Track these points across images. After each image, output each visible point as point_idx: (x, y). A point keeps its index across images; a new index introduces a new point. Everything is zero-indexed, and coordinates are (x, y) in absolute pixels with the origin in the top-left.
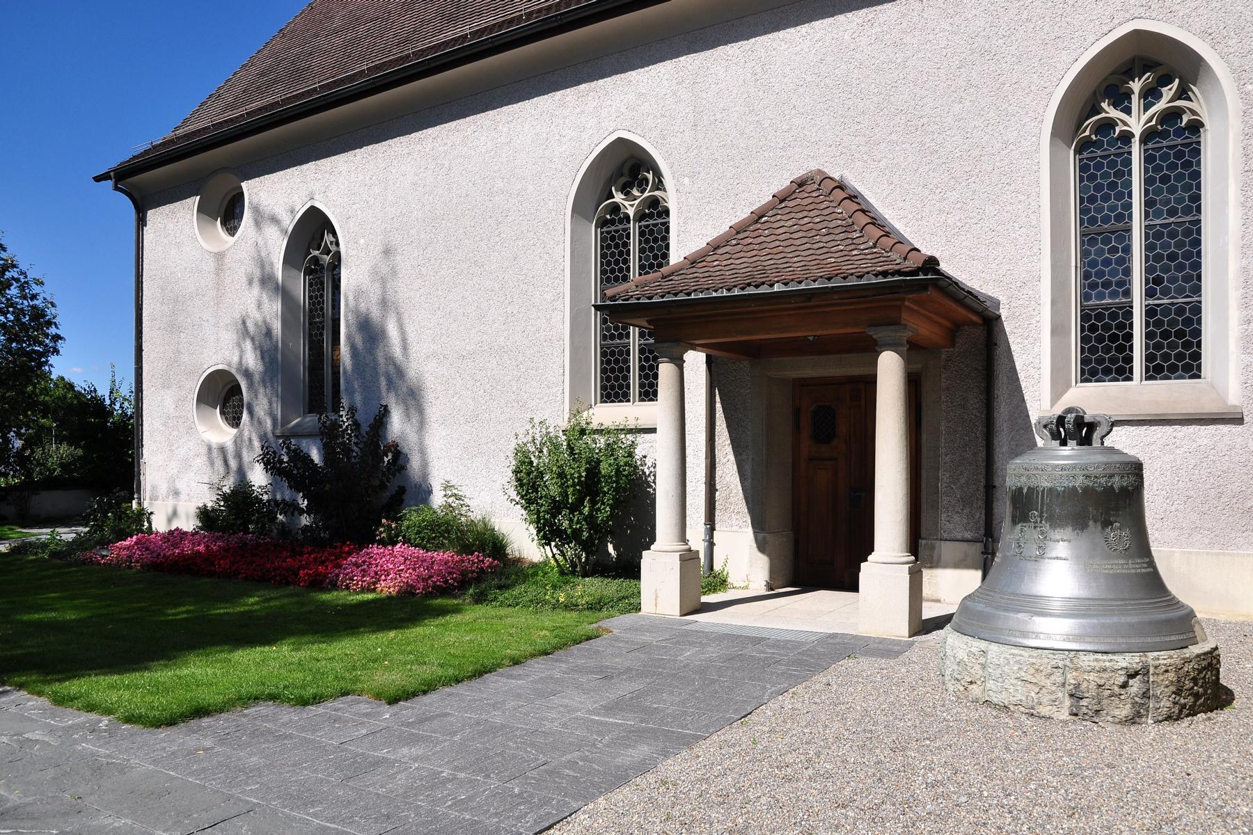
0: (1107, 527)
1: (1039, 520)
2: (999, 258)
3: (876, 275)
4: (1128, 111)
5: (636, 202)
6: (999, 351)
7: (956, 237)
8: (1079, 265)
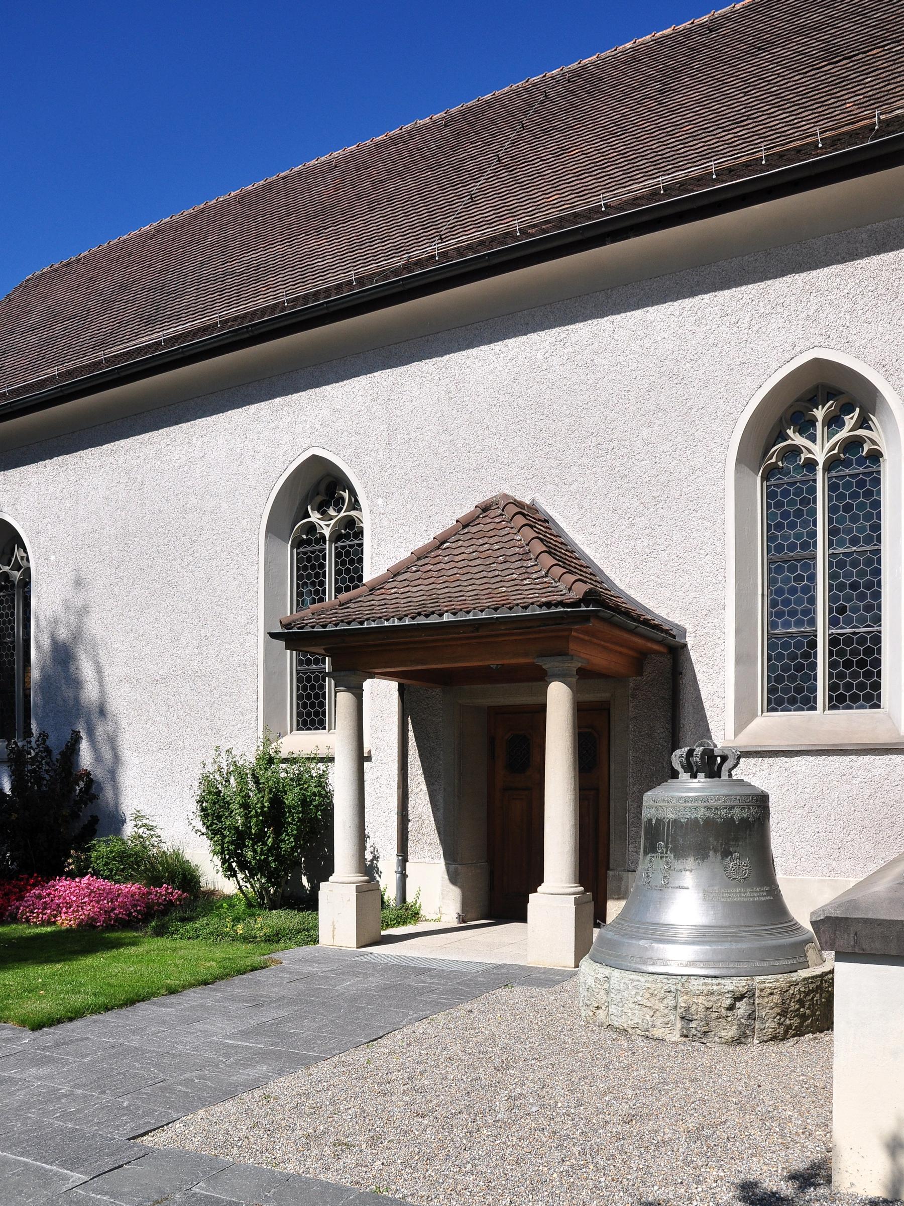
0: (727, 857)
1: (665, 850)
2: (687, 586)
3: (540, 606)
4: (814, 440)
5: (332, 522)
6: (685, 680)
7: (644, 563)
8: (766, 593)
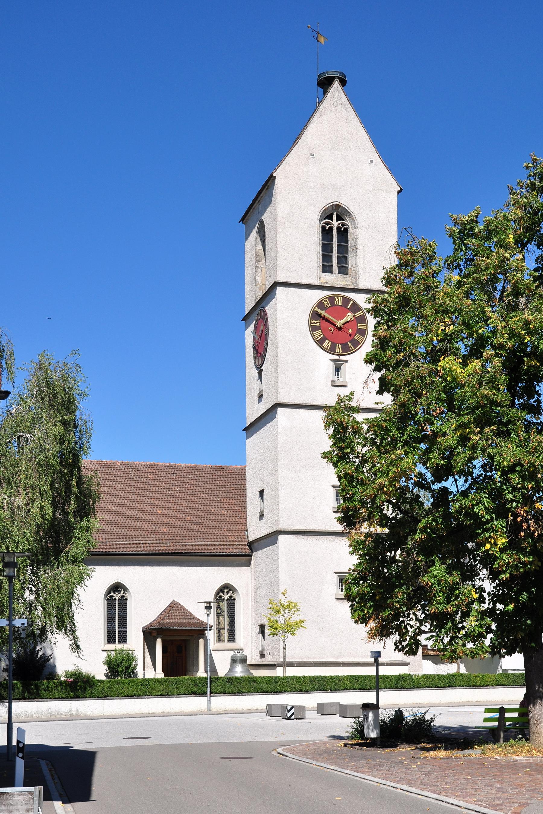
4: (224, 594)
